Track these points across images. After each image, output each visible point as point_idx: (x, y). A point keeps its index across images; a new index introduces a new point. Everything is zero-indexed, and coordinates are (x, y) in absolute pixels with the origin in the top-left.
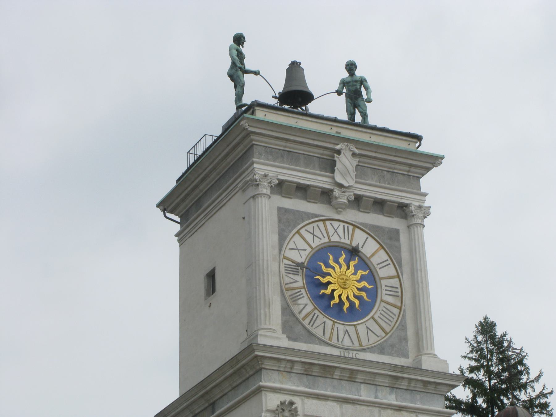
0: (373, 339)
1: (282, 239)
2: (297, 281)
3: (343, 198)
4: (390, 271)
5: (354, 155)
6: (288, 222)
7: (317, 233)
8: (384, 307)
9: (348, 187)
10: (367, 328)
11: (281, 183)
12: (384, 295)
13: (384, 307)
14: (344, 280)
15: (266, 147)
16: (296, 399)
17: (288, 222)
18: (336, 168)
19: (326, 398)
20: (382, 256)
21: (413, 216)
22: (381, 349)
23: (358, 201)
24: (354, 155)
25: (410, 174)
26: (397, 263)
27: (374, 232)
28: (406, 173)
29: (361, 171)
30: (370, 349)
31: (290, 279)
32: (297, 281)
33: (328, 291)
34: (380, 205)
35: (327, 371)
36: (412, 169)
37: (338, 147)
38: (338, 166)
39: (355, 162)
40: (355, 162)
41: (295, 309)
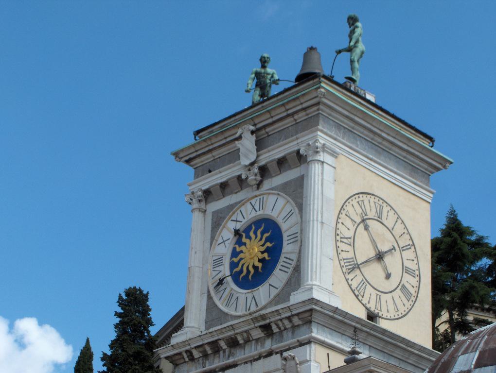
0: (274, 292)
2: (220, 271)
3: (253, 177)
5: (252, 132)
7: (240, 218)
8: (285, 257)
9: (252, 164)
10: (270, 285)
13: (285, 257)
14: (254, 250)
15: (203, 165)
18: (240, 154)
21: (306, 156)
23: (264, 171)
24: (252, 132)
25: (310, 116)
28: (306, 117)
29: (260, 145)
31: (216, 272)
32: (220, 271)
33: (260, 265)
34: (282, 163)
36: (309, 111)
37: (237, 135)
38: (242, 150)
39: (254, 138)
40: (254, 138)
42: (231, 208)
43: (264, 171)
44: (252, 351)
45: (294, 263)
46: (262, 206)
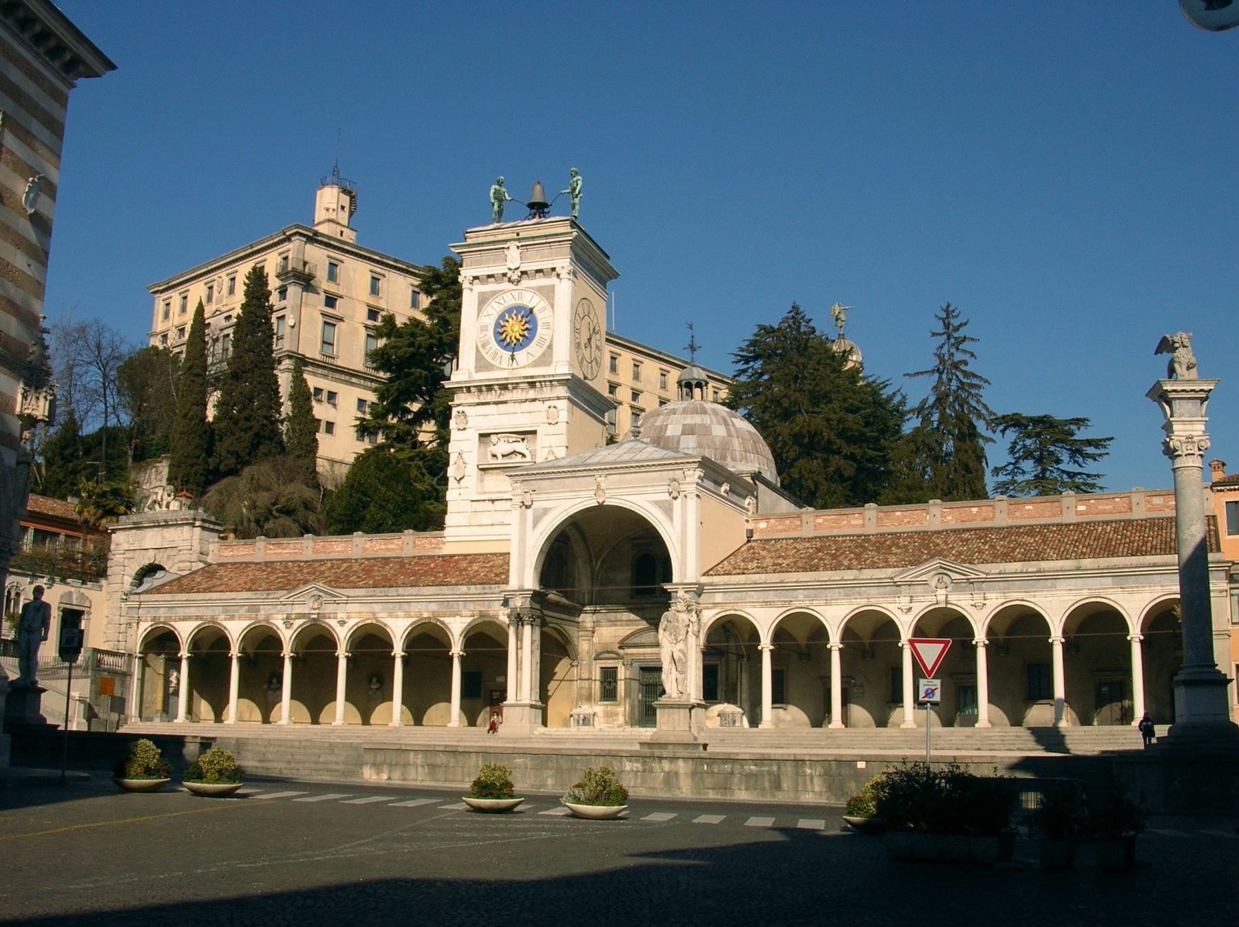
1: (479, 311)
3: (515, 277)
4: (548, 311)
6: (483, 300)
11: (476, 278)
12: (540, 331)
14: (514, 328)
16: (466, 409)
17: (483, 300)
19: (488, 403)
20: (544, 304)
22: (535, 364)
26: (552, 306)
27: (540, 290)
30: (529, 366)
35: (490, 388)
41: (483, 353)
42: (494, 293)
43: (523, 273)
44: (518, 395)
45: (548, 343)
46: (520, 297)
